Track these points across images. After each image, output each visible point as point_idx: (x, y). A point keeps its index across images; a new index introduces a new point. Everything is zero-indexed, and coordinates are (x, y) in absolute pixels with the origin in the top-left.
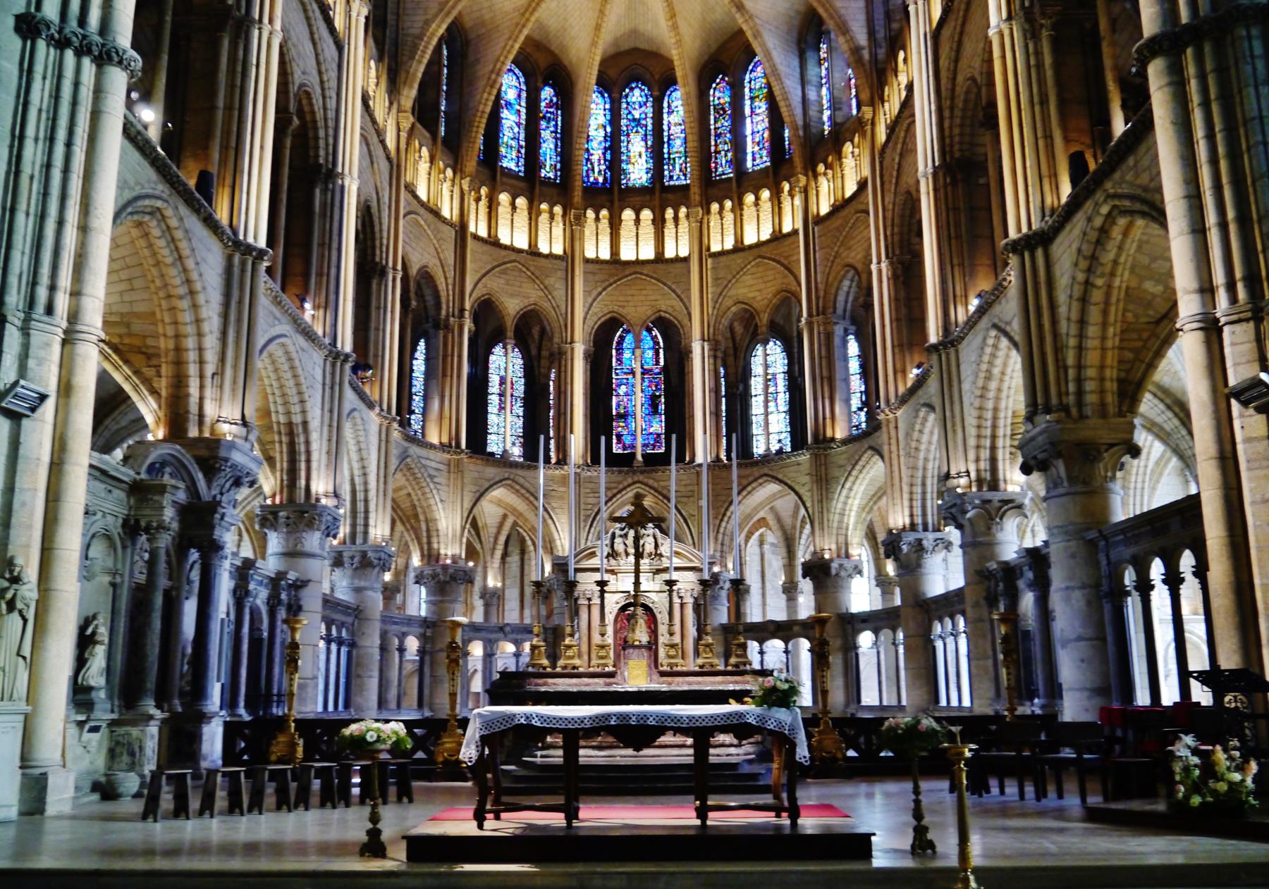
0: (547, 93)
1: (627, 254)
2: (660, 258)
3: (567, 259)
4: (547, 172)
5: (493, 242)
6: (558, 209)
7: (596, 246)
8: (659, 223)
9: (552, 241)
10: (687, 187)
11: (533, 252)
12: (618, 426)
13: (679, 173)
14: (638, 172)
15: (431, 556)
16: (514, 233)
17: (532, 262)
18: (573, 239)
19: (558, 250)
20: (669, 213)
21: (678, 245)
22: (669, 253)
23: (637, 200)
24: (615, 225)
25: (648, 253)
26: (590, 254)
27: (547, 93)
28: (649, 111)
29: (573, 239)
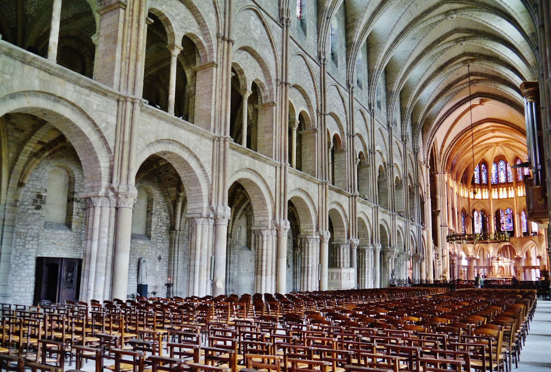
0: (483, 166)
1: (501, 197)
2: (508, 198)
3: (489, 199)
4: (484, 181)
5: (474, 199)
6: (487, 190)
7: (495, 195)
8: (507, 190)
9: (486, 195)
10: (512, 183)
11: (482, 199)
12: (502, 225)
13: (511, 180)
14: (503, 180)
15: (467, 255)
16: (478, 196)
17: (482, 201)
18: (490, 195)
19: (487, 198)
20: (509, 188)
21: (511, 194)
22: (510, 197)
23: (502, 186)
24: (498, 191)
25: (505, 197)
26: (494, 198)
27: (483, 166)
28: (504, 166)
29: (490, 195)
